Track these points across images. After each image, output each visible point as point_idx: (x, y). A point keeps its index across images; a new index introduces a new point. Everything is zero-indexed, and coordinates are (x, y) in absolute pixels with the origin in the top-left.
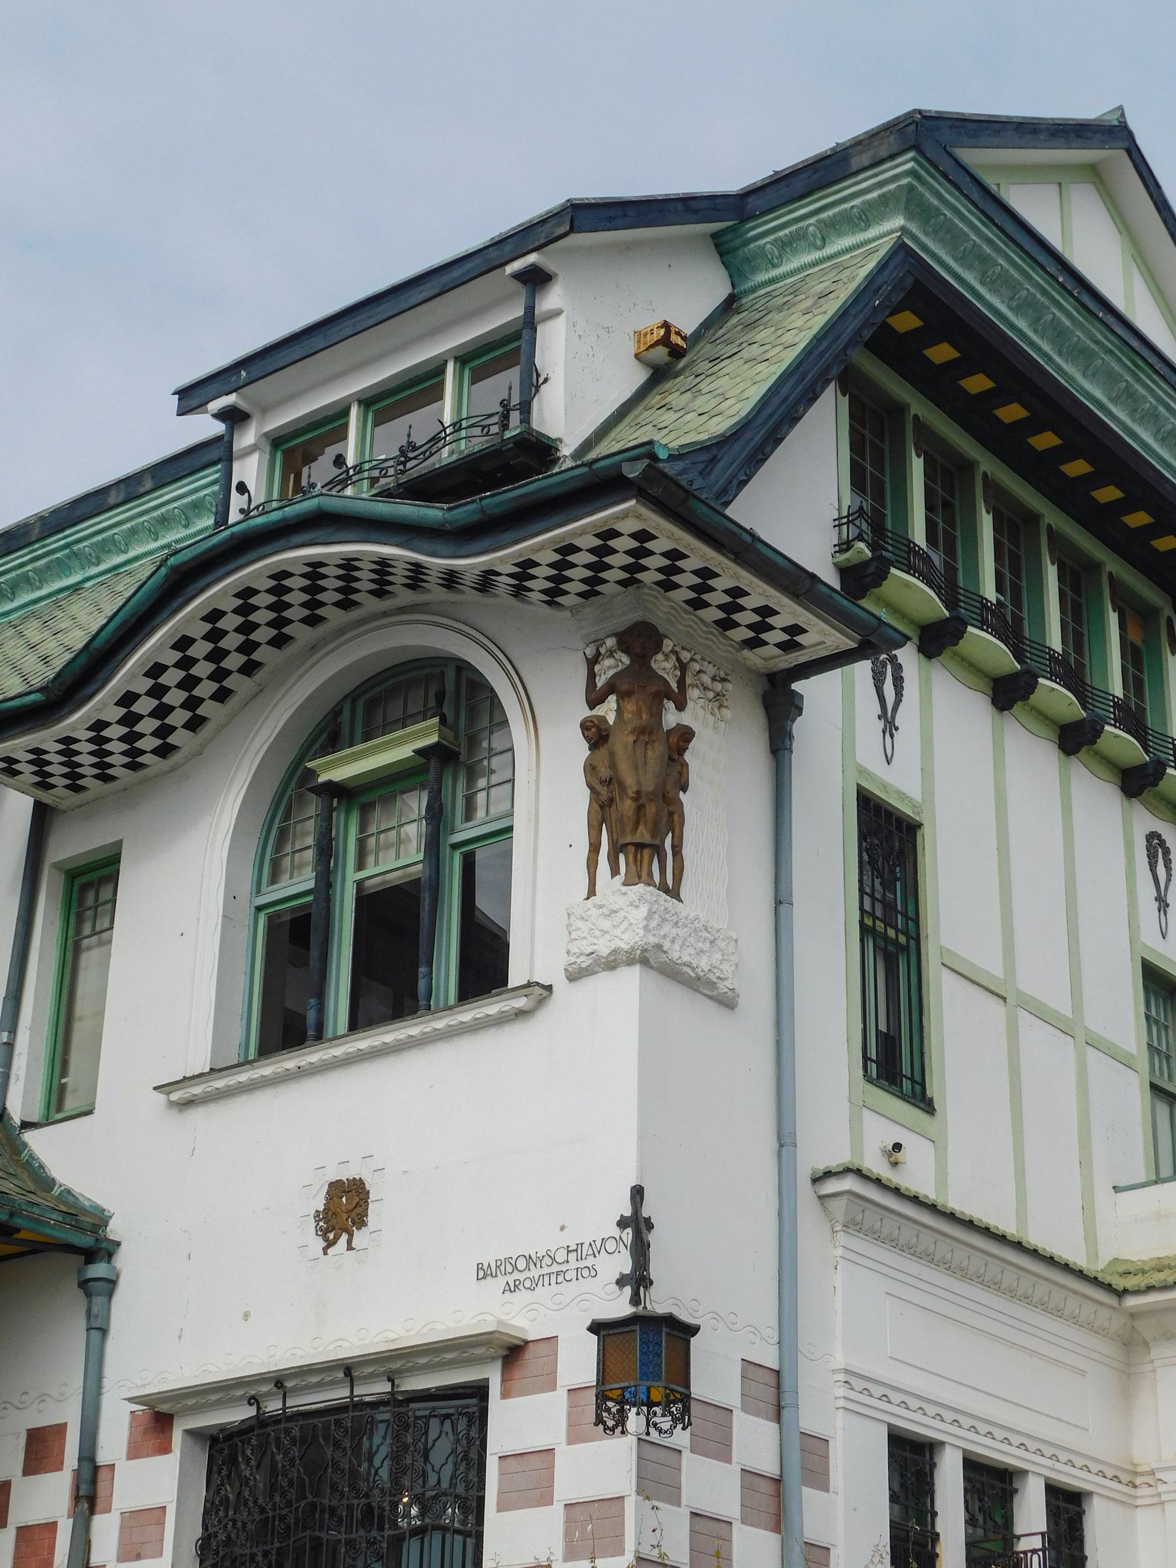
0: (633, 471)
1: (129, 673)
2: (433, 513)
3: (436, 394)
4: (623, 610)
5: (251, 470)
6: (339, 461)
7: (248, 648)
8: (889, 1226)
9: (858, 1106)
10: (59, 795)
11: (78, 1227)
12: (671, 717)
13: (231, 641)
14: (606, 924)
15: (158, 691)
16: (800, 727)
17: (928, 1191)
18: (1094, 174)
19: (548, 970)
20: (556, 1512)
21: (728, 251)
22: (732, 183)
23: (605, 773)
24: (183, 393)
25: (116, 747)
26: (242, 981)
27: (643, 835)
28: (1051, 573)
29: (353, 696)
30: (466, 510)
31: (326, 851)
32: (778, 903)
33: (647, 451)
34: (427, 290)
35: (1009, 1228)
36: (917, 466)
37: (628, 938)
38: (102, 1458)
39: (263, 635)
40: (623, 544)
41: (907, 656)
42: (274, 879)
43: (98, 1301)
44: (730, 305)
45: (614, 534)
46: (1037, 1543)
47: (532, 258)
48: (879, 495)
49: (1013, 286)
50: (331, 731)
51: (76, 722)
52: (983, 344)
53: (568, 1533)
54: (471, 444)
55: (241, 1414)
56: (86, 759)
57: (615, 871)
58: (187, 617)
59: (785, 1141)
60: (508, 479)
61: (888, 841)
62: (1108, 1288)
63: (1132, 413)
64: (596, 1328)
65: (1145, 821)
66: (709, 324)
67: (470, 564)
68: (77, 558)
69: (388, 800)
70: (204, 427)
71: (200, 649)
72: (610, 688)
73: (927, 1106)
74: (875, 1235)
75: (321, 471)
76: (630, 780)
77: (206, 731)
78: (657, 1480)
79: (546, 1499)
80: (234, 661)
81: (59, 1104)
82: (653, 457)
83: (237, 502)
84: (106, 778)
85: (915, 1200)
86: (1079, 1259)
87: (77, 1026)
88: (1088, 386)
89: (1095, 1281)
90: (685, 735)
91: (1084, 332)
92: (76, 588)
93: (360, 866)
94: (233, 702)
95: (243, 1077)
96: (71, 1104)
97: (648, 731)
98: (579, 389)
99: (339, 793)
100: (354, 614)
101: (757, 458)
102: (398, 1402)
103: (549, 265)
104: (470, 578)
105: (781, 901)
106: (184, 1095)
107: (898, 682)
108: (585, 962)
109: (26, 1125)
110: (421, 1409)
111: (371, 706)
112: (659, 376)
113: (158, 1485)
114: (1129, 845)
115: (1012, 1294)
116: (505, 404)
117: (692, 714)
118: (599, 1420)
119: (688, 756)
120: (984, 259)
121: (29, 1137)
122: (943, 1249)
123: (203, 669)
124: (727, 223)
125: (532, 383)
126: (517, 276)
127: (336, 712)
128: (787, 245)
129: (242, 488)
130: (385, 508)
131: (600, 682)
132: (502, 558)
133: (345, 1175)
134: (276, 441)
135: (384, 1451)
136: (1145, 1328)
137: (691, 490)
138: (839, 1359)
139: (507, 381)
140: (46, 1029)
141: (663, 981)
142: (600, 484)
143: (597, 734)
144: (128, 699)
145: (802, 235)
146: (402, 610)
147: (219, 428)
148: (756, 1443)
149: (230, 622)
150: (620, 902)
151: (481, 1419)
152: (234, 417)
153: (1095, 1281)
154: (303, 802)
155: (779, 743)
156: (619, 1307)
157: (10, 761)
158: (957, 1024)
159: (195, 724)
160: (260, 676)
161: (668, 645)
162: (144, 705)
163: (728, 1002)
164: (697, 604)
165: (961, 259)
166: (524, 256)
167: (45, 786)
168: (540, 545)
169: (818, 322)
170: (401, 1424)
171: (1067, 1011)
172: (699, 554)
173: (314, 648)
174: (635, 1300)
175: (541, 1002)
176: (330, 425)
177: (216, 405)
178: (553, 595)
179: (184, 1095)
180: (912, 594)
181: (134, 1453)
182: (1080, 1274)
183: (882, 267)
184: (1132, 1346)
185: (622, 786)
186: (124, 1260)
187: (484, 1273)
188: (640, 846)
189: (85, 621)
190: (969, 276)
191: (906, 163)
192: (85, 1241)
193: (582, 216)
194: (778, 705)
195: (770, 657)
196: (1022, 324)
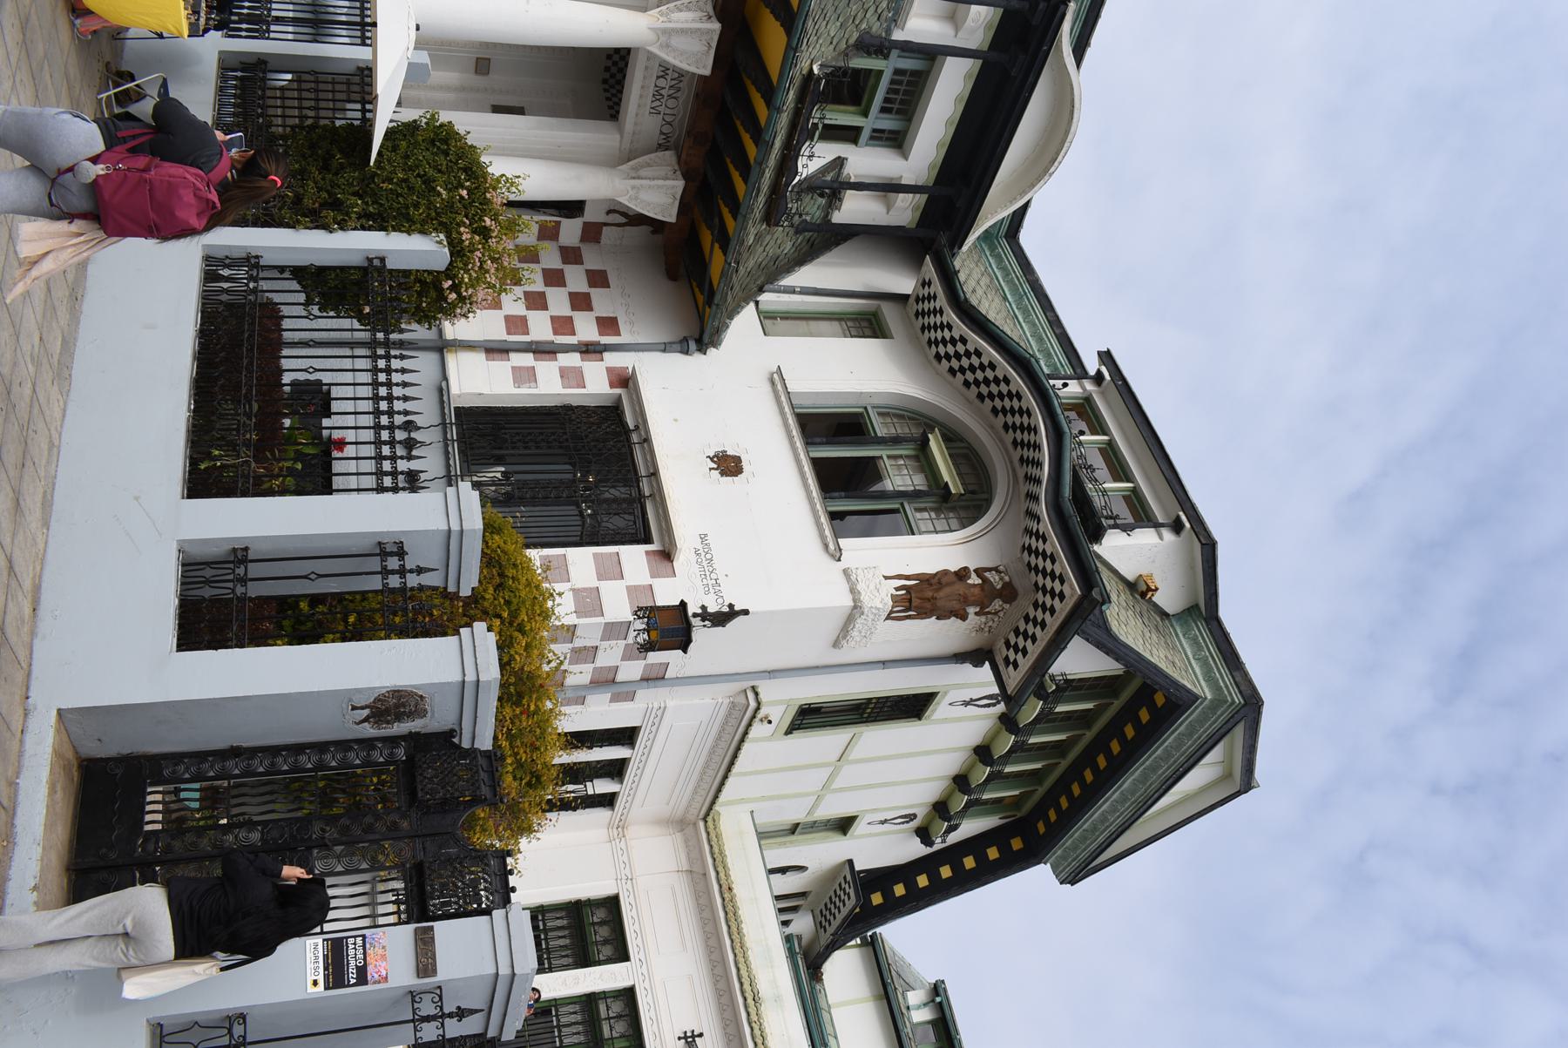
0: (1095, 593)
1: (976, 340)
2: (1067, 491)
3: (1116, 479)
4: (1023, 583)
5: (1074, 388)
6: (1082, 433)
7: (991, 396)
8: (733, 722)
10: (913, 307)
11: (712, 335)
12: (971, 610)
13: (994, 389)
14: (872, 587)
15: (968, 354)
16: (968, 667)
17: (752, 733)
18: (1227, 776)
19: (848, 559)
20: (594, 583)
21: (1190, 612)
22: (1224, 613)
23: (944, 581)
24: (1108, 353)
25: (939, 335)
26: (832, 403)
27: (916, 602)
28: (1038, 766)
29: (970, 447)
30: (1069, 508)
31: (895, 441)
32: (884, 663)
33: (1106, 599)
34: (1168, 473)
35: (735, 770)
36: (1089, 706)
37: (867, 600)
38: (606, 355)
39: (998, 403)
40: (1057, 586)
41: (1001, 707)
42: (880, 414)
43: (678, 347)
44: (1164, 615)
45: (1053, 562)
46: (590, 792)
47: (1188, 525)
48: (1076, 689)
49: (1178, 748)
50: (952, 438)
51: (951, 316)
52: (1148, 736)
53: (585, 589)
54: (1098, 502)
55: (630, 421)
56: (932, 320)
57: (897, 589)
58: (1005, 368)
59: (772, 673)
60: (1082, 522)
61: (913, 707)
62: (707, 814)
64: (683, 604)
65: (921, 813)
66: (1155, 605)
67: (1043, 509)
68: (1020, 298)
69: (922, 470)
70: (1092, 365)
71: (990, 374)
72: (985, 580)
73: (789, 732)
74: (729, 715)
75: (1072, 415)
76: (941, 594)
77: (949, 377)
78: (613, 630)
79: (601, 577)
80: (984, 390)
81: (768, 318)
82: (1103, 603)
83: (1059, 383)
84: (923, 329)
85: (746, 733)
86: (723, 797)
87: (804, 323)
89: (710, 809)
90: (964, 617)
91: (1155, 780)
92: (1005, 298)
93: (889, 457)
94: (964, 389)
95: (787, 409)
96: (767, 323)
97: (966, 601)
98: (1127, 551)
99: (924, 444)
100: (1010, 447)
101: (1099, 645)
102: (640, 500)
103: (1184, 534)
104: (1033, 506)
105: (884, 664)
106: (777, 380)
107: (988, 706)
108: (853, 578)
109: (757, 303)
110: (638, 512)
111: (966, 456)
112: (1131, 586)
113: (596, 384)
114: (911, 806)
115: (703, 773)
116: (1117, 517)
117: (973, 619)
118: (640, 609)
120: (1191, 735)
121: (752, 305)
122: (723, 745)
123: (980, 375)
124: (1203, 610)
125: (1127, 529)
126: (1178, 517)
127: (962, 440)
128: (1194, 642)
129: (1065, 385)
130: (1067, 467)
131: (987, 574)
132: (1047, 526)
133: (744, 464)
134: (1088, 400)
135: (617, 494)
136: (689, 830)
137: (1085, 617)
138: (670, 704)
139: (1126, 516)
140: (802, 308)
142: (1087, 571)
143: (962, 574)
144: (963, 340)
145: (1200, 648)
146: (1014, 470)
147: (1092, 372)
149: (1004, 388)
150: (883, 594)
151: (638, 542)
152: (1098, 379)
153: (710, 809)
154: (917, 426)
155: (959, 657)
156: (692, 609)
157: (930, 284)
158: (828, 741)
159: (952, 371)
160: (977, 402)
161: (1007, 606)
162: (960, 348)
163: (836, 644)
164: (1027, 619)
166: (1186, 520)
167: (917, 300)
168: (1054, 545)
169: (1163, 665)
170: (630, 501)
171: (834, 786)
172: (1053, 623)
173: (992, 427)
174: (695, 615)
175: (832, 556)
176: (1098, 426)
177: (1104, 370)
178: (1029, 549)
179: (777, 380)
180: (1032, 709)
181: (609, 370)
182: (713, 803)
183: (1189, 691)
184: (681, 824)
185: (938, 590)
186: (697, 358)
187: (703, 537)
188: (910, 601)
189: (1008, 328)
190: (1182, 728)
191: (1238, 699)
192: (706, 339)
193: (1209, 548)
194: (975, 656)
195: (1001, 652)
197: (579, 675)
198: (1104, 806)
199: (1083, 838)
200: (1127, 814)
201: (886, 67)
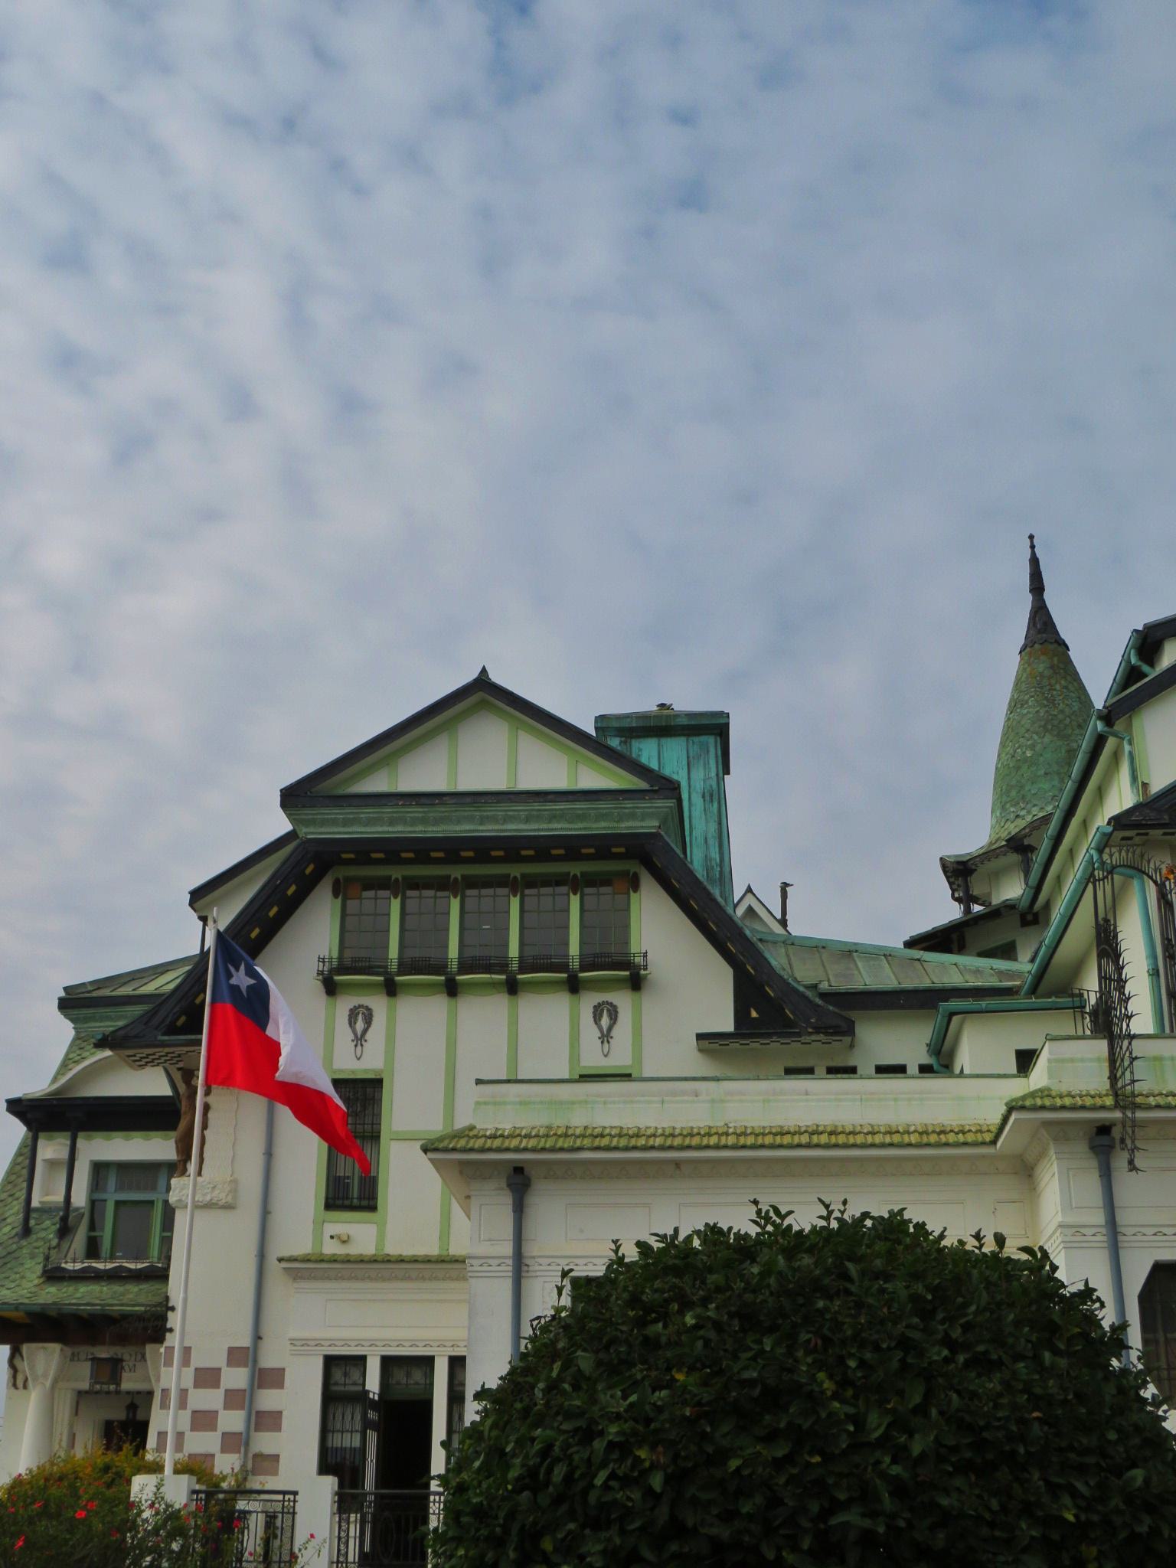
9: (319, 1225)
18: (482, 705)
59: (262, 1256)
65: (589, 1001)
88: (458, 828)
91: (438, 811)
105: (269, 1154)
107: (368, 1021)
148: (236, 1378)
163: (229, 1207)
165: (344, 826)
196: (400, 828)
197: (233, 1421)
198: (512, 828)
199: (582, 818)
200: (504, 806)
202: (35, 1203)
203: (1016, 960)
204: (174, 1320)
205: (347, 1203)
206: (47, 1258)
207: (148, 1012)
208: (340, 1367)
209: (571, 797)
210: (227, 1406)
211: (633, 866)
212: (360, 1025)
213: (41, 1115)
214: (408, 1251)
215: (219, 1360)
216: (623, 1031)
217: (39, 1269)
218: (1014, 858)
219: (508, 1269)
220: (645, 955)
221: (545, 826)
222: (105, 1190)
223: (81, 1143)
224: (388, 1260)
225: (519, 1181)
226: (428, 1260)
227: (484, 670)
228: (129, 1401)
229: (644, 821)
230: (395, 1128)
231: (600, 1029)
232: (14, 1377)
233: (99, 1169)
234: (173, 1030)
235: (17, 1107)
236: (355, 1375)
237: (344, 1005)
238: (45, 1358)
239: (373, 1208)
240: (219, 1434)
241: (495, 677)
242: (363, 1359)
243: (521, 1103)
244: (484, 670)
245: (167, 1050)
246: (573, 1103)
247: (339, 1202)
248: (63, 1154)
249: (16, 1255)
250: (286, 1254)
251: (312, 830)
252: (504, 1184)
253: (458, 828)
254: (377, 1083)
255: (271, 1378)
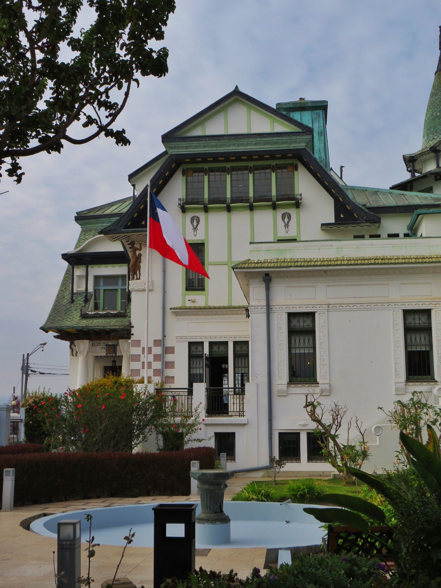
9: (184, 296)
12: (138, 253)
59: (164, 307)
63: (244, 146)
65: (280, 213)
88: (229, 148)
90: (140, 255)
91: (222, 142)
119: (142, 257)
141: (137, 292)
148: (158, 350)
161: (136, 242)
197: (157, 365)
199: (275, 143)
200: (246, 140)
201: (102, 288)
202: (75, 291)
203: (432, 193)
204: (133, 331)
205: (193, 288)
206: (81, 310)
207: (117, 220)
208: (194, 347)
209: (272, 135)
210: (155, 360)
211: (295, 161)
212: (195, 223)
213: (74, 259)
214: (216, 305)
215: (151, 344)
216: (293, 222)
217: (79, 314)
218: (433, 154)
219: (264, 310)
220: (301, 195)
221: (262, 147)
222: (99, 286)
223: (89, 269)
224: (210, 308)
225: (267, 279)
226: (225, 308)
227: (237, 87)
228: (112, 359)
229: (299, 144)
230: (210, 261)
231: (285, 222)
232: (72, 352)
233: (97, 278)
234: (126, 227)
235: (65, 257)
236: (200, 349)
237: (189, 216)
238: (83, 345)
239: (203, 290)
240: (152, 370)
241: (241, 89)
242: (202, 343)
243: (267, 250)
244: (237, 87)
245: (125, 234)
246: (286, 250)
247: (191, 288)
248: (84, 273)
249: (70, 309)
250: (173, 307)
251: (174, 151)
252: (262, 280)
253: (229, 148)
254: (203, 244)
255: (170, 350)
